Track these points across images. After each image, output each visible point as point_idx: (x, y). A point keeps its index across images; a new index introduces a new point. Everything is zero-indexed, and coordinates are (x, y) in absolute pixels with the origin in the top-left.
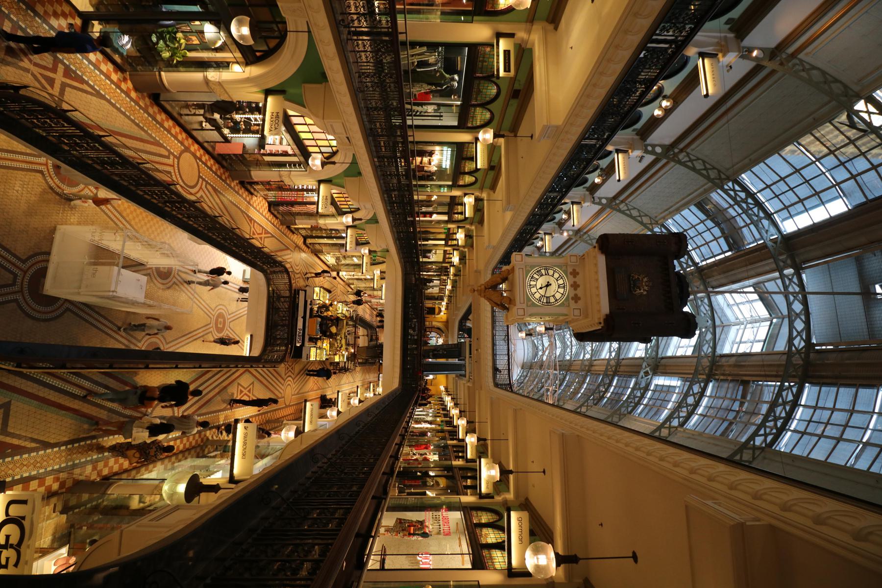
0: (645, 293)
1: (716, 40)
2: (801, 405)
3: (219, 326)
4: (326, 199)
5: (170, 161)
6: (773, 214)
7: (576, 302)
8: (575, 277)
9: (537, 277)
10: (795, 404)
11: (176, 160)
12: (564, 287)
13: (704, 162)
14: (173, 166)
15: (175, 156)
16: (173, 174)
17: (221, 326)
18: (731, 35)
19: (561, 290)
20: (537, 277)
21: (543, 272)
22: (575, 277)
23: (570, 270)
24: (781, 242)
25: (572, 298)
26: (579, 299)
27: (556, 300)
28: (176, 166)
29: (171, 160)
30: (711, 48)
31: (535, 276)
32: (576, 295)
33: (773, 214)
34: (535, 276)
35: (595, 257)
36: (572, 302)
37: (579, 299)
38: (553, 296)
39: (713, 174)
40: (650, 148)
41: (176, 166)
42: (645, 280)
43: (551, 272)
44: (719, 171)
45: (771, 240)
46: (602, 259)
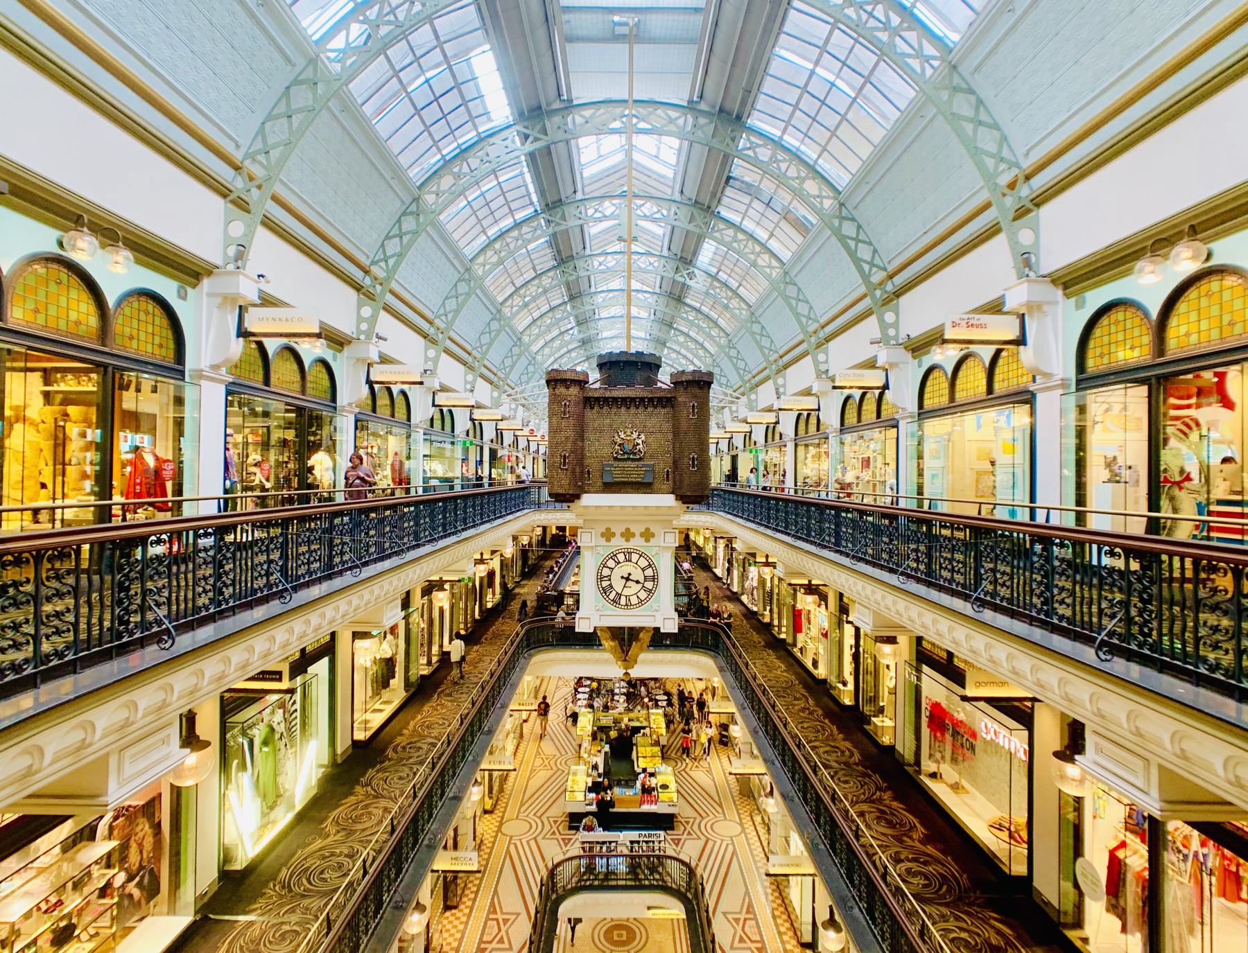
0: (643, 437)
1: (216, 311)
2: (781, 138)
3: (624, 938)
4: (456, 859)
6: (479, 134)
7: (653, 535)
8: (613, 535)
9: (613, 594)
10: (778, 144)
12: (630, 553)
13: (387, 237)
17: (624, 933)
18: (206, 282)
19: (635, 557)
20: (613, 594)
21: (605, 584)
22: (613, 535)
23: (603, 541)
24: (526, 127)
25: (647, 540)
26: (647, 529)
27: (650, 566)
30: (229, 317)
31: (612, 596)
32: (642, 535)
33: (479, 134)
34: (612, 596)
35: (586, 507)
36: (653, 541)
37: (647, 529)
38: (643, 570)
39: (409, 224)
40: (364, 326)
42: (623, 436)
43: (606, 572)
44: (404, 214)
45: (523, 144)
46: (588, 499)
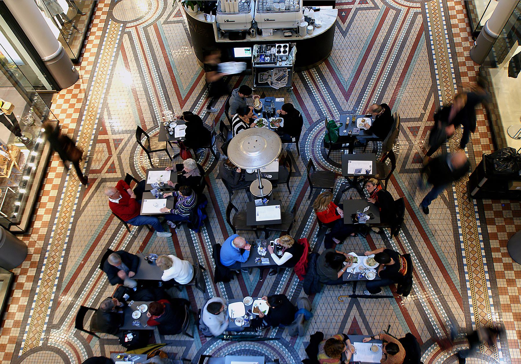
5: (133, 31)
11: (128, 25)
14: (136, 26)
15: (124, 27)
16: (144, 25)
28: (135, 23)
29: (130, 29)
41: (135, 23)
